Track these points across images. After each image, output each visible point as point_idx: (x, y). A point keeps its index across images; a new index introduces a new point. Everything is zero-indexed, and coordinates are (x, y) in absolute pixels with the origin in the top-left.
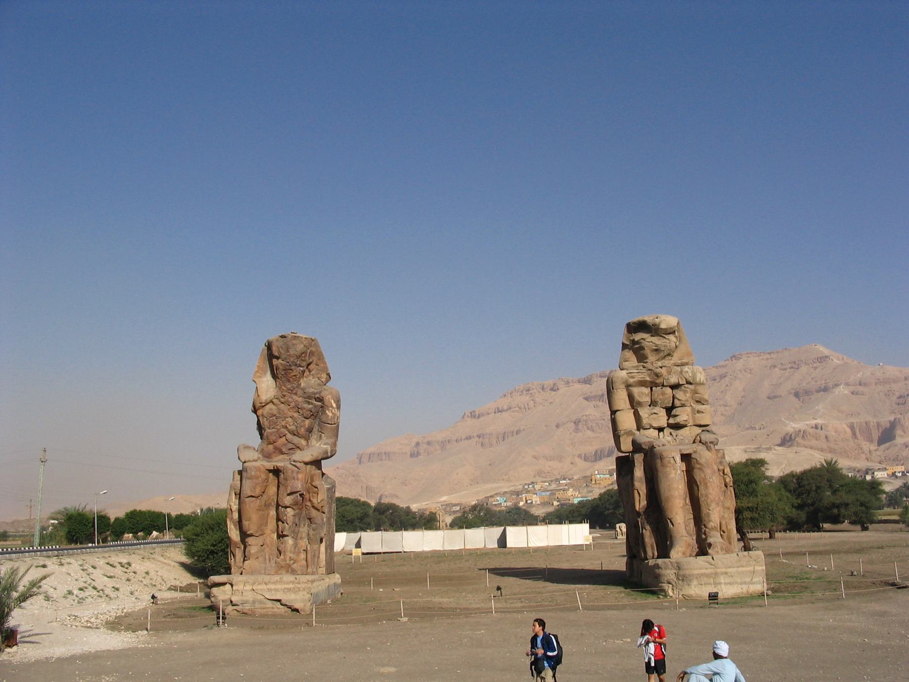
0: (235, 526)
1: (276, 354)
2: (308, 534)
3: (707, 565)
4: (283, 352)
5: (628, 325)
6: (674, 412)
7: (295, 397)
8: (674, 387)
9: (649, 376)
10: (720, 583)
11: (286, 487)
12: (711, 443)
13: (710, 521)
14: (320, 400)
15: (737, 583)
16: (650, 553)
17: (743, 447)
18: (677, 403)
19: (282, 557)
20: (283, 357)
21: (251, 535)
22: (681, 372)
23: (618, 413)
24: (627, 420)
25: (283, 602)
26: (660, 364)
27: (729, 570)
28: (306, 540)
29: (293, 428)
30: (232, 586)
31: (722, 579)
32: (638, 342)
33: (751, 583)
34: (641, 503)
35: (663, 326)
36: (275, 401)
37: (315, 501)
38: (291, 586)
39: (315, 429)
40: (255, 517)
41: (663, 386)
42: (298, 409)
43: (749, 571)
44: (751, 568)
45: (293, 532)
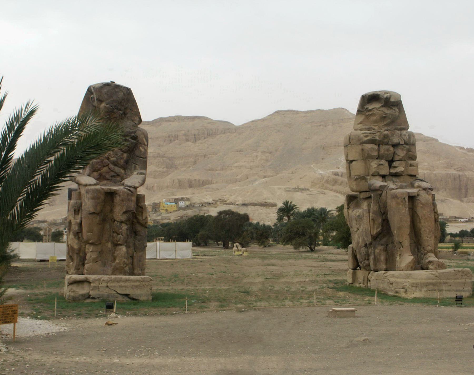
2: (134, 244)
5: (363, 97)
6: (395, 164)
8: (395, 146)
10: (442, 290)
12: (430, 189)
13: (429, 245)
14: (135, 138)
15: (453, 290)
17: (285, 187)
18: (397, 158)
19: (117, 261)
22: (401, 135)
25: (131, 296)
26: (386, 128)
27: (448, 281)
28: (132, 248)
31: (444, 288)
33: (462, 291)
35: (392, 100)
37: (140, 218)
38: (138, 284)
41: (387, 144)
43: (462, 283)
44: (463, 281)
45: (126, 242)
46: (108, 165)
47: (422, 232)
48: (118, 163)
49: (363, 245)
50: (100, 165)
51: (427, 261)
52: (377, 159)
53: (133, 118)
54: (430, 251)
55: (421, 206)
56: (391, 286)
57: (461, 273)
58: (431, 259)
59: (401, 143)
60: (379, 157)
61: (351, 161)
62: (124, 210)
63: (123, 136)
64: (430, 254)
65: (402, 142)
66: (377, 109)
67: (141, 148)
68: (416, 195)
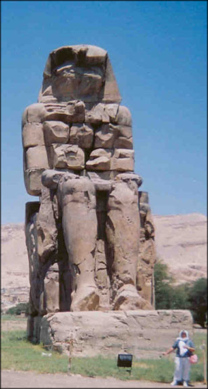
3: (117, 322)
5: (52, 55)
6: (94, 153)
8: (98, 125)
9: (71, 110)
13: (126, 272)
16: (50, 307)
23: (31, 148)
24: (38, 156)
35: (89, 54)
47: (116, 249)
51: (119, 296)
52: (67, 143)
54: (130, 282)
55: (117, 206)
56: (52, 338)
57: (170, 317)
58: (124, 294)
59: (103, 121)
64: (126, 286)
65: (106, 119)
66: (68, 70)
68: (110, 188)
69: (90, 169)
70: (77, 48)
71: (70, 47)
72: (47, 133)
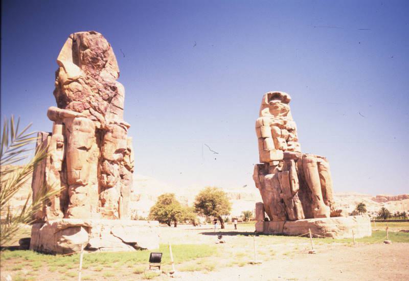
0: (56, 174)
1: (86, 44)
2: (121, 188)
4: (92, 44)
6: (289, 143)
7: (96, 81)
11: (115, 144)
13: (333, 199)
19: (106, 205)
20: (93, 48)
21: (80, 184)
25: (139, 245)
29: (95, 104)
30: (88, 229)
32: (275, 104)
34: (296, 187)
36: (80, 80)
39: (108, 110)
40: (85, 166)
41: (285, 128)
42: (99, 92)
46: (88, 109)
47: (327, 189)
48: (99, 109)
49: (279, 200)
50: (81, 107)
53: (111, 72)
55: (325, 169)
56: (320, 231)
60: (282, 136)
61: (265, 138)
62: (118, 148)
63: (103, 84)
65: (293, 129)
66: (278, 103)
67: (119, 98)
69: (288, 150)
70: (283, 94)
71: (279, 92)
72: (273, 131)
